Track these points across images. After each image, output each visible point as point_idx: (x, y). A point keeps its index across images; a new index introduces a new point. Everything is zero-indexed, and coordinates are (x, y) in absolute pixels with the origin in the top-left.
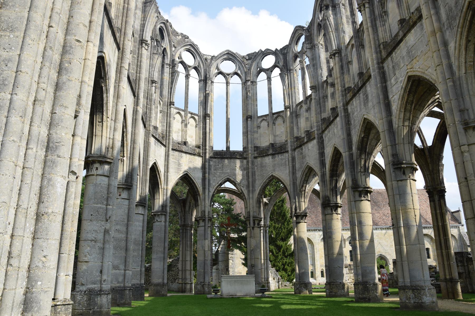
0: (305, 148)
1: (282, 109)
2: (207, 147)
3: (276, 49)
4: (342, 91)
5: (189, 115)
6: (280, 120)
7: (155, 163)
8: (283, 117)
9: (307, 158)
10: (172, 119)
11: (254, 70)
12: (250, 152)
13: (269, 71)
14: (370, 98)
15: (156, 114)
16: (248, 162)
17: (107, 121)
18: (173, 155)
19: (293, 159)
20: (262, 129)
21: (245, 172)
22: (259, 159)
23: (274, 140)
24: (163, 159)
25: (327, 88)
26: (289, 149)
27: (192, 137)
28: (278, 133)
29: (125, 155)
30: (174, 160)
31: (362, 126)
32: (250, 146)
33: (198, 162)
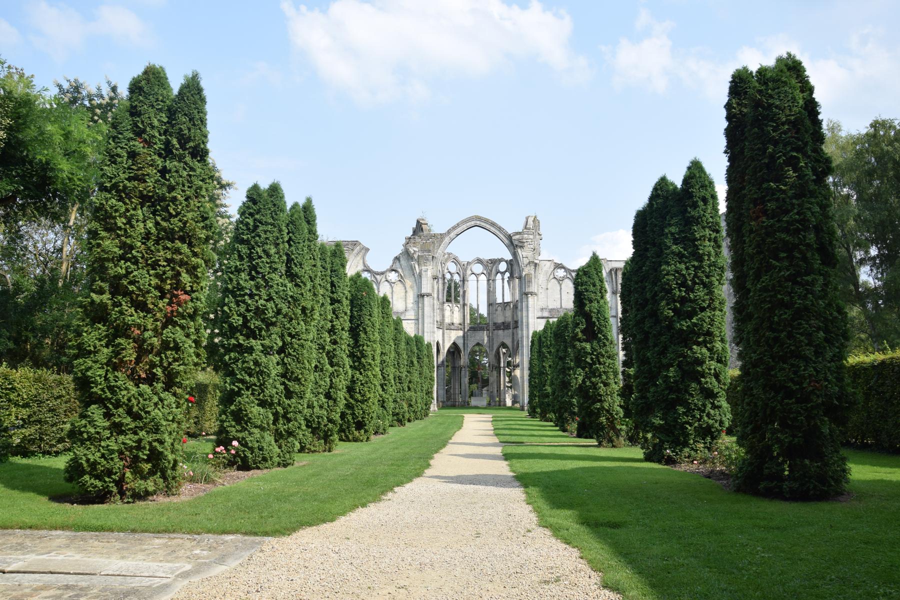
6: (508, 308)
11: (494, 271)
13: (503, 273)
33: (461, 333)
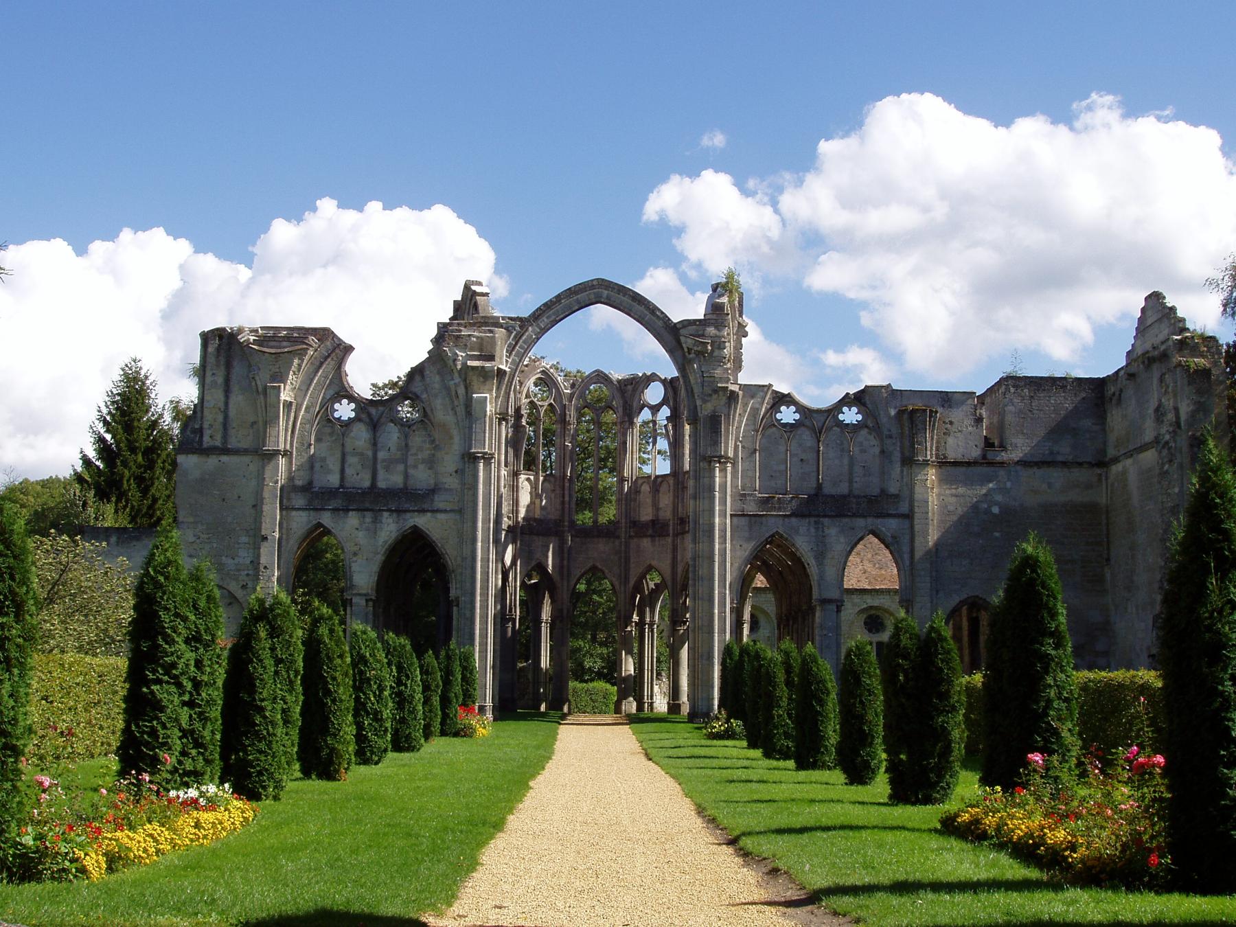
19: (675, 550)
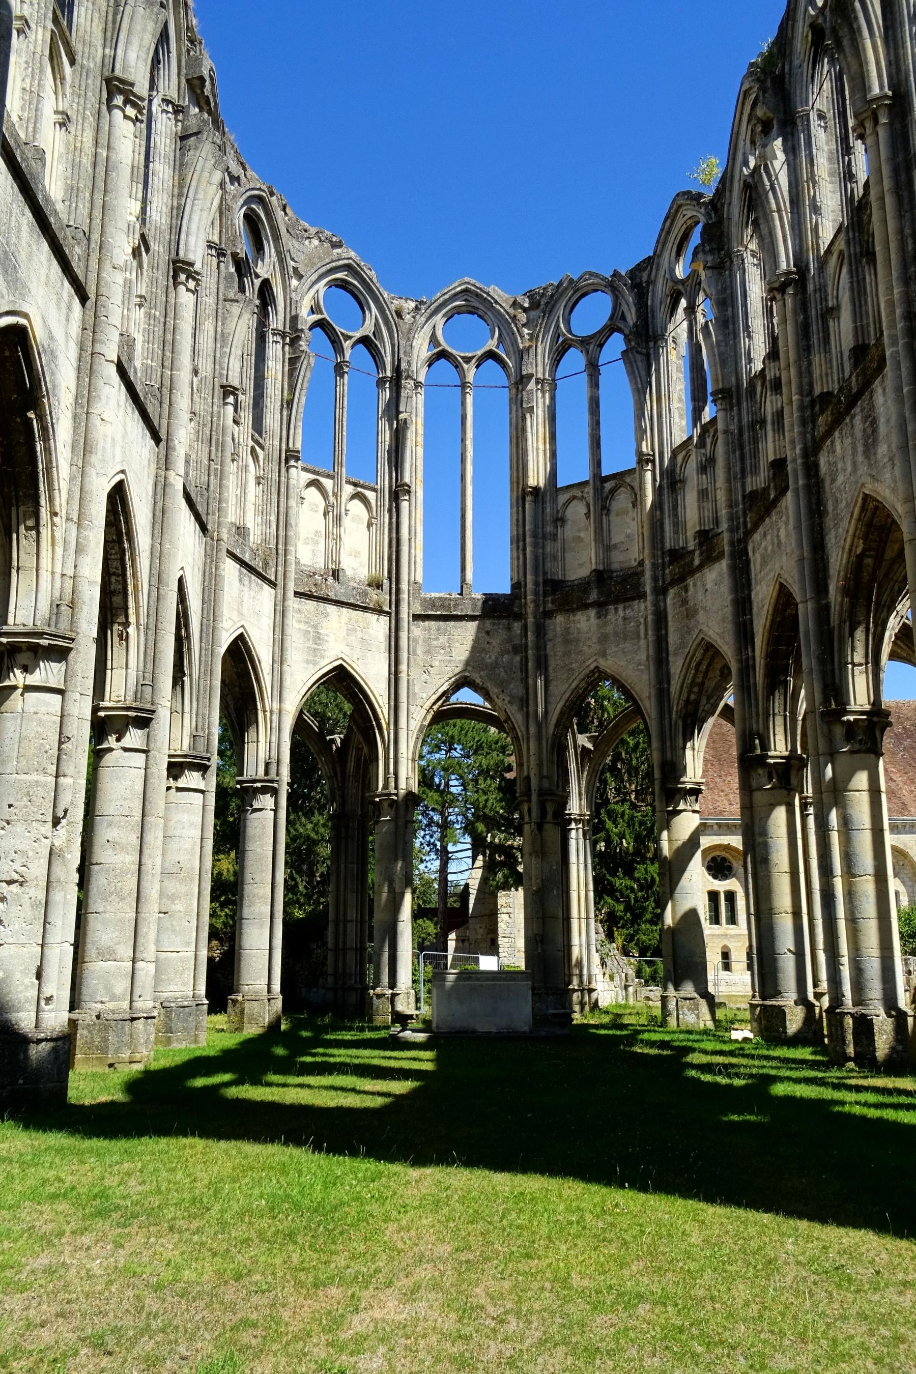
0: (695, 585)
1: (632, 464)
2: (404, 586)
3: (616, 274)
4: (802, 408)
5: (349, 490)
7: (241, 637)
8: (632, 488)
9: (701, 617)
10: (292, 503)
12: (530, 597)
13: (592, 345)
14: (883, 429)
15: (243, 486)
16: (525, 628)
17: (53, 524)
18: (299, 611)
19: (661, 619)
20: (568, 526)
21: (518, 658)
22: (560, 619)
23: (607, 560)
24: (267, 621)
25: (764, 395)
26: (648, 589)
27: (357, 554)
28: (616, 538)
29: (132, 619)
30: (303, 626)
31: (859, 520)
32: (530, 578)
